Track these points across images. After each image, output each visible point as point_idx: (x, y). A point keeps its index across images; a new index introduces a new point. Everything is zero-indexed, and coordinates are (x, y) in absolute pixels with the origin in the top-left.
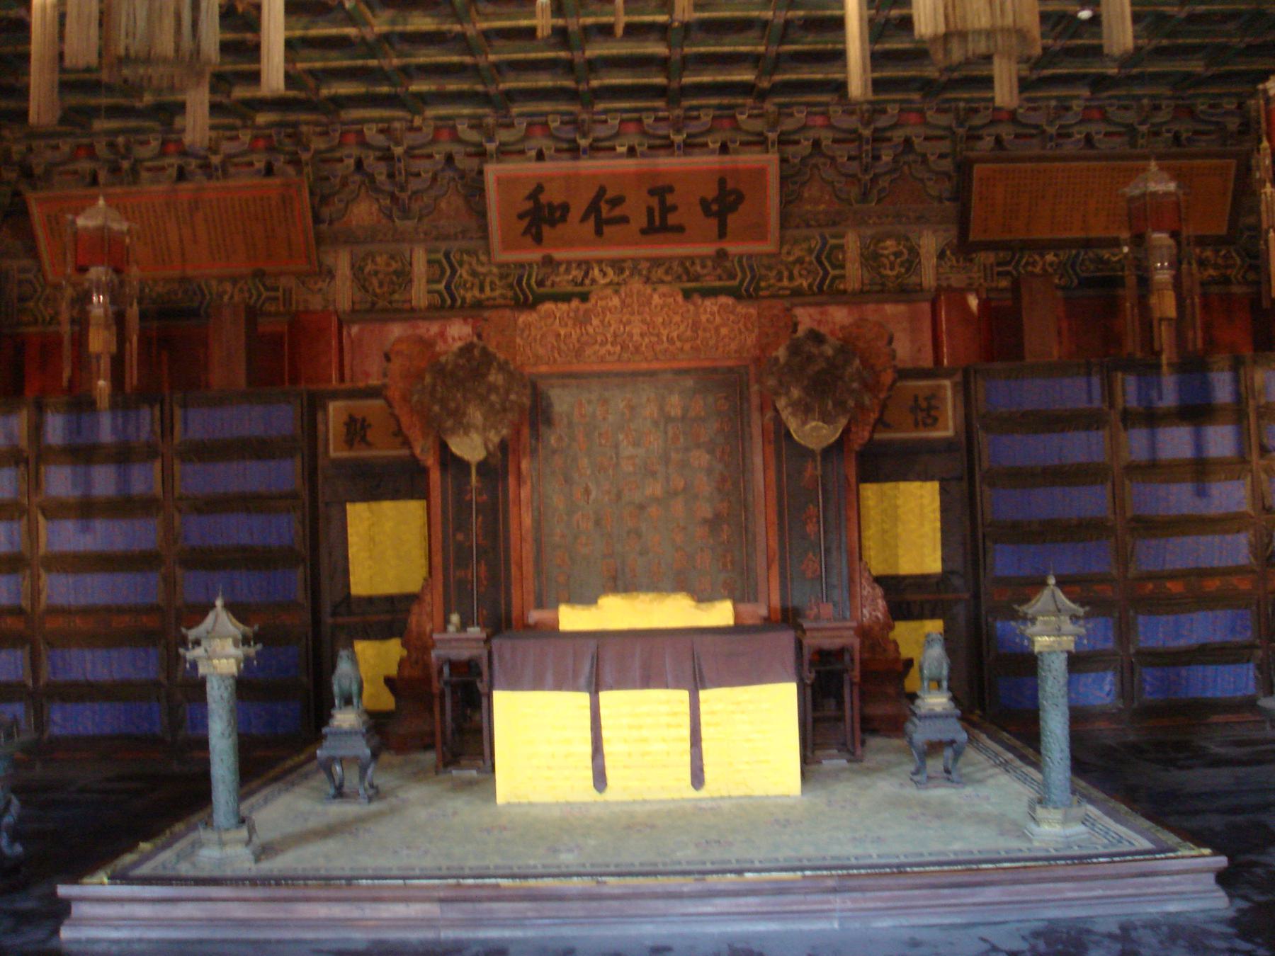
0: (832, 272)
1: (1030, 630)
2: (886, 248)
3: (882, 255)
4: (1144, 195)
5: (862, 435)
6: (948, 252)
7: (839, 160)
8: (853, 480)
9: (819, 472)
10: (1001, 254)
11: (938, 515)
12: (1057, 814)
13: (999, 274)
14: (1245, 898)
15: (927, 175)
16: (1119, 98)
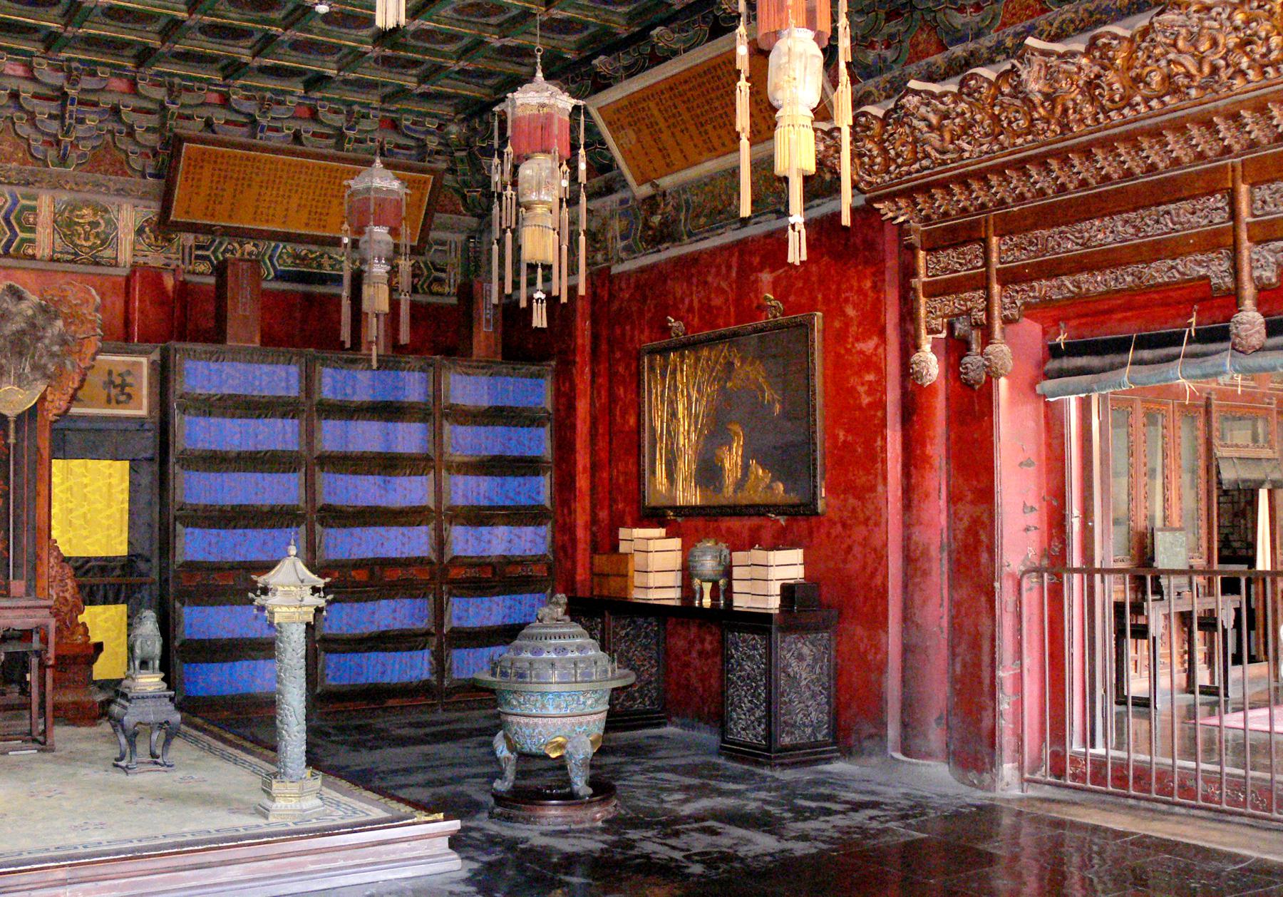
0: (21, 235)
1: (269, 601)
2: (82, 217)
3: (78, 224)
4: (368, 190)
5: (57, 403)
6: (147, 229)
7: (39, 117)
8: (46, 453)
9: (12, 440)
10: (201, 238)
11: (126, 496)
12: (294, 788)
13: (197, 257)
14: (471, 859)
15: (132, 148)
16: (330, 100)
